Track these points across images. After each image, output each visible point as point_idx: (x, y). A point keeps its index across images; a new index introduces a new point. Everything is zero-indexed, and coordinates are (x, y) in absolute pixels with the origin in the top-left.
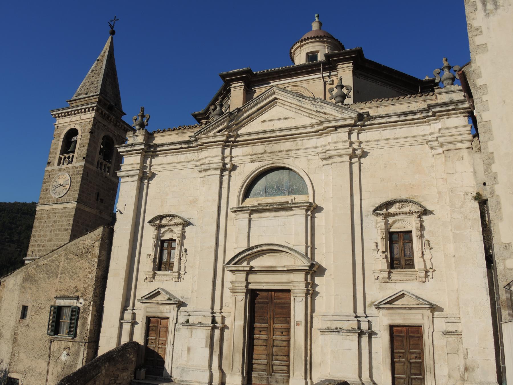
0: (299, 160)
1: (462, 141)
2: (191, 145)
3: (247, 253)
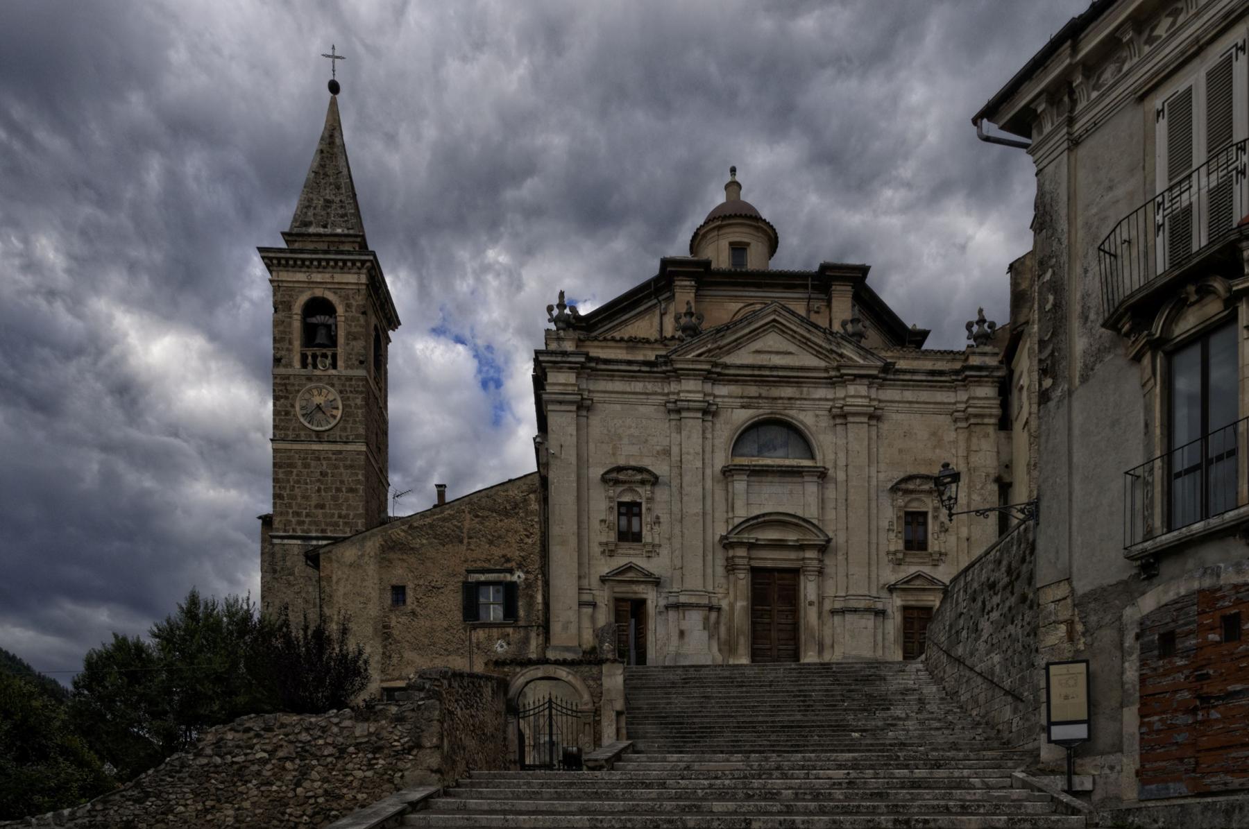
0: (804, 413)
1: (991, 416)
2: (655, 369)
3: (752, 522)
